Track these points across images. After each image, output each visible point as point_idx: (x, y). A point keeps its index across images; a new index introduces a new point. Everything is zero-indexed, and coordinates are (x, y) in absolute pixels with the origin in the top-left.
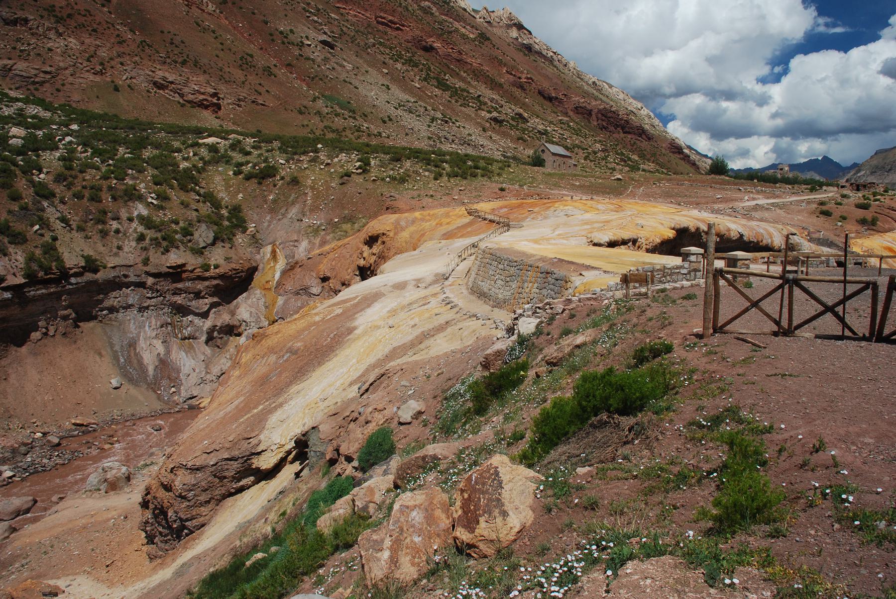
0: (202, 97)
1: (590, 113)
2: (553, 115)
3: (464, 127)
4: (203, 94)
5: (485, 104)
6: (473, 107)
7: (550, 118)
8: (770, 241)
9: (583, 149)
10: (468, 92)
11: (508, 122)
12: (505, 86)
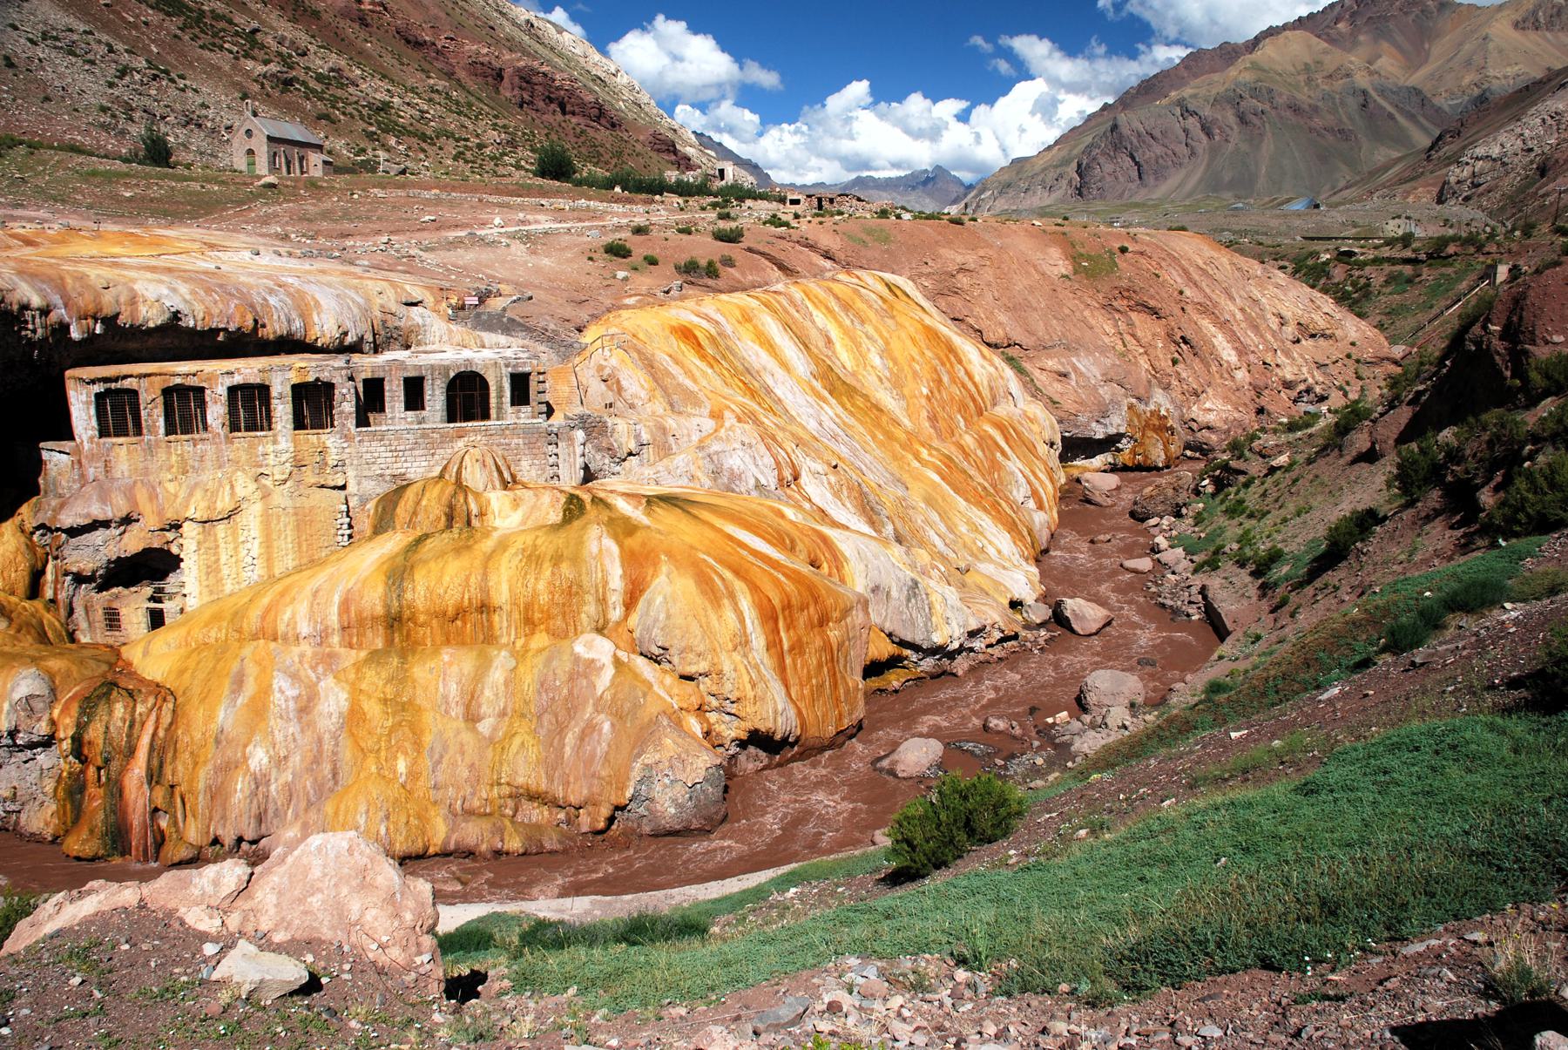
1: (499, 75)
2: (420, 75)
3: (196, 91)
5: (262, 47)
6: (231, 52)
7: (411, 82)
8: (297, 324)
9: (457, 140)
10: (230, 22)
11: (304, 83)
12: (324, 16)
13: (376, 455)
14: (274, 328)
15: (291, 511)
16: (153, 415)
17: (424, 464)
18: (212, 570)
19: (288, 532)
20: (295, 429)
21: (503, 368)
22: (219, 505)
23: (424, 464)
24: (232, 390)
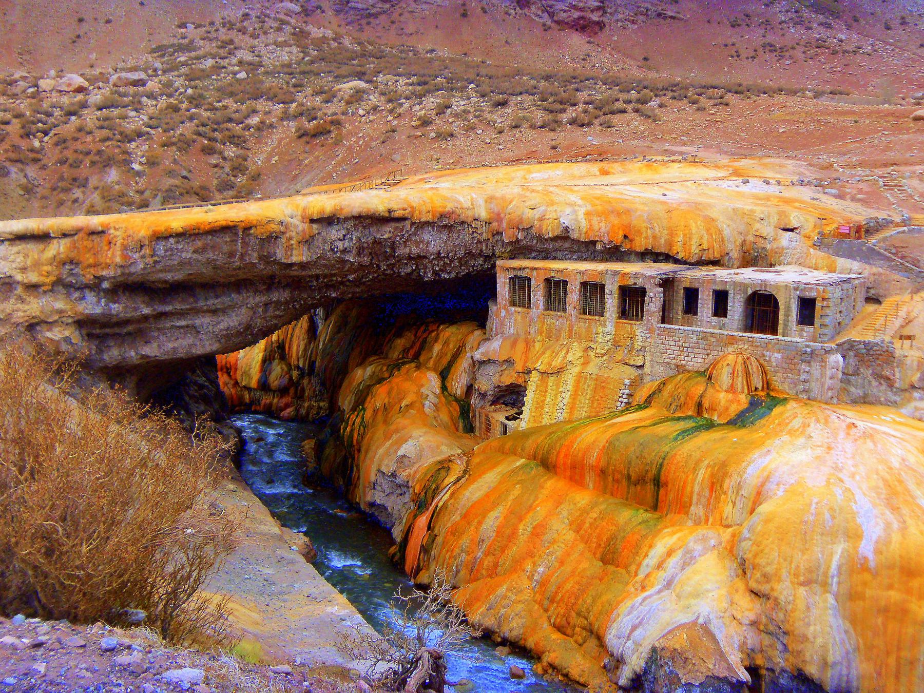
0: (576, 14)
4: (581, 9)
13: (668, 347)
14: (640, 244)
15: (594, 376)
16: (538, 296)
17: (700, 360)
18: (540, 406)
19: (589, 392)
20: (619, 318)
21: (792, 291)
22: (554, 363)
23: (700, 360)
24: (584, 285)
